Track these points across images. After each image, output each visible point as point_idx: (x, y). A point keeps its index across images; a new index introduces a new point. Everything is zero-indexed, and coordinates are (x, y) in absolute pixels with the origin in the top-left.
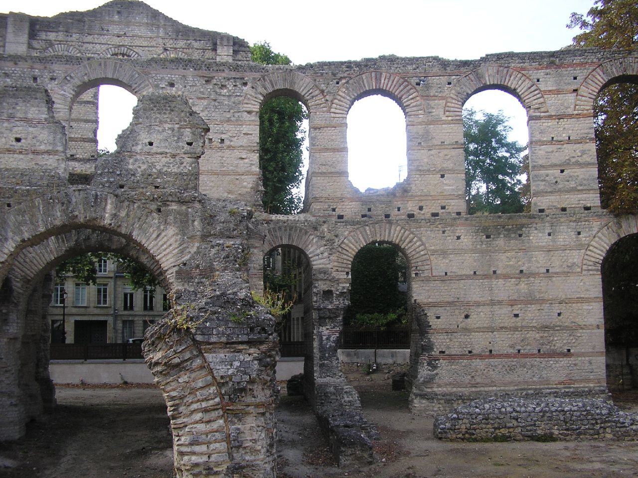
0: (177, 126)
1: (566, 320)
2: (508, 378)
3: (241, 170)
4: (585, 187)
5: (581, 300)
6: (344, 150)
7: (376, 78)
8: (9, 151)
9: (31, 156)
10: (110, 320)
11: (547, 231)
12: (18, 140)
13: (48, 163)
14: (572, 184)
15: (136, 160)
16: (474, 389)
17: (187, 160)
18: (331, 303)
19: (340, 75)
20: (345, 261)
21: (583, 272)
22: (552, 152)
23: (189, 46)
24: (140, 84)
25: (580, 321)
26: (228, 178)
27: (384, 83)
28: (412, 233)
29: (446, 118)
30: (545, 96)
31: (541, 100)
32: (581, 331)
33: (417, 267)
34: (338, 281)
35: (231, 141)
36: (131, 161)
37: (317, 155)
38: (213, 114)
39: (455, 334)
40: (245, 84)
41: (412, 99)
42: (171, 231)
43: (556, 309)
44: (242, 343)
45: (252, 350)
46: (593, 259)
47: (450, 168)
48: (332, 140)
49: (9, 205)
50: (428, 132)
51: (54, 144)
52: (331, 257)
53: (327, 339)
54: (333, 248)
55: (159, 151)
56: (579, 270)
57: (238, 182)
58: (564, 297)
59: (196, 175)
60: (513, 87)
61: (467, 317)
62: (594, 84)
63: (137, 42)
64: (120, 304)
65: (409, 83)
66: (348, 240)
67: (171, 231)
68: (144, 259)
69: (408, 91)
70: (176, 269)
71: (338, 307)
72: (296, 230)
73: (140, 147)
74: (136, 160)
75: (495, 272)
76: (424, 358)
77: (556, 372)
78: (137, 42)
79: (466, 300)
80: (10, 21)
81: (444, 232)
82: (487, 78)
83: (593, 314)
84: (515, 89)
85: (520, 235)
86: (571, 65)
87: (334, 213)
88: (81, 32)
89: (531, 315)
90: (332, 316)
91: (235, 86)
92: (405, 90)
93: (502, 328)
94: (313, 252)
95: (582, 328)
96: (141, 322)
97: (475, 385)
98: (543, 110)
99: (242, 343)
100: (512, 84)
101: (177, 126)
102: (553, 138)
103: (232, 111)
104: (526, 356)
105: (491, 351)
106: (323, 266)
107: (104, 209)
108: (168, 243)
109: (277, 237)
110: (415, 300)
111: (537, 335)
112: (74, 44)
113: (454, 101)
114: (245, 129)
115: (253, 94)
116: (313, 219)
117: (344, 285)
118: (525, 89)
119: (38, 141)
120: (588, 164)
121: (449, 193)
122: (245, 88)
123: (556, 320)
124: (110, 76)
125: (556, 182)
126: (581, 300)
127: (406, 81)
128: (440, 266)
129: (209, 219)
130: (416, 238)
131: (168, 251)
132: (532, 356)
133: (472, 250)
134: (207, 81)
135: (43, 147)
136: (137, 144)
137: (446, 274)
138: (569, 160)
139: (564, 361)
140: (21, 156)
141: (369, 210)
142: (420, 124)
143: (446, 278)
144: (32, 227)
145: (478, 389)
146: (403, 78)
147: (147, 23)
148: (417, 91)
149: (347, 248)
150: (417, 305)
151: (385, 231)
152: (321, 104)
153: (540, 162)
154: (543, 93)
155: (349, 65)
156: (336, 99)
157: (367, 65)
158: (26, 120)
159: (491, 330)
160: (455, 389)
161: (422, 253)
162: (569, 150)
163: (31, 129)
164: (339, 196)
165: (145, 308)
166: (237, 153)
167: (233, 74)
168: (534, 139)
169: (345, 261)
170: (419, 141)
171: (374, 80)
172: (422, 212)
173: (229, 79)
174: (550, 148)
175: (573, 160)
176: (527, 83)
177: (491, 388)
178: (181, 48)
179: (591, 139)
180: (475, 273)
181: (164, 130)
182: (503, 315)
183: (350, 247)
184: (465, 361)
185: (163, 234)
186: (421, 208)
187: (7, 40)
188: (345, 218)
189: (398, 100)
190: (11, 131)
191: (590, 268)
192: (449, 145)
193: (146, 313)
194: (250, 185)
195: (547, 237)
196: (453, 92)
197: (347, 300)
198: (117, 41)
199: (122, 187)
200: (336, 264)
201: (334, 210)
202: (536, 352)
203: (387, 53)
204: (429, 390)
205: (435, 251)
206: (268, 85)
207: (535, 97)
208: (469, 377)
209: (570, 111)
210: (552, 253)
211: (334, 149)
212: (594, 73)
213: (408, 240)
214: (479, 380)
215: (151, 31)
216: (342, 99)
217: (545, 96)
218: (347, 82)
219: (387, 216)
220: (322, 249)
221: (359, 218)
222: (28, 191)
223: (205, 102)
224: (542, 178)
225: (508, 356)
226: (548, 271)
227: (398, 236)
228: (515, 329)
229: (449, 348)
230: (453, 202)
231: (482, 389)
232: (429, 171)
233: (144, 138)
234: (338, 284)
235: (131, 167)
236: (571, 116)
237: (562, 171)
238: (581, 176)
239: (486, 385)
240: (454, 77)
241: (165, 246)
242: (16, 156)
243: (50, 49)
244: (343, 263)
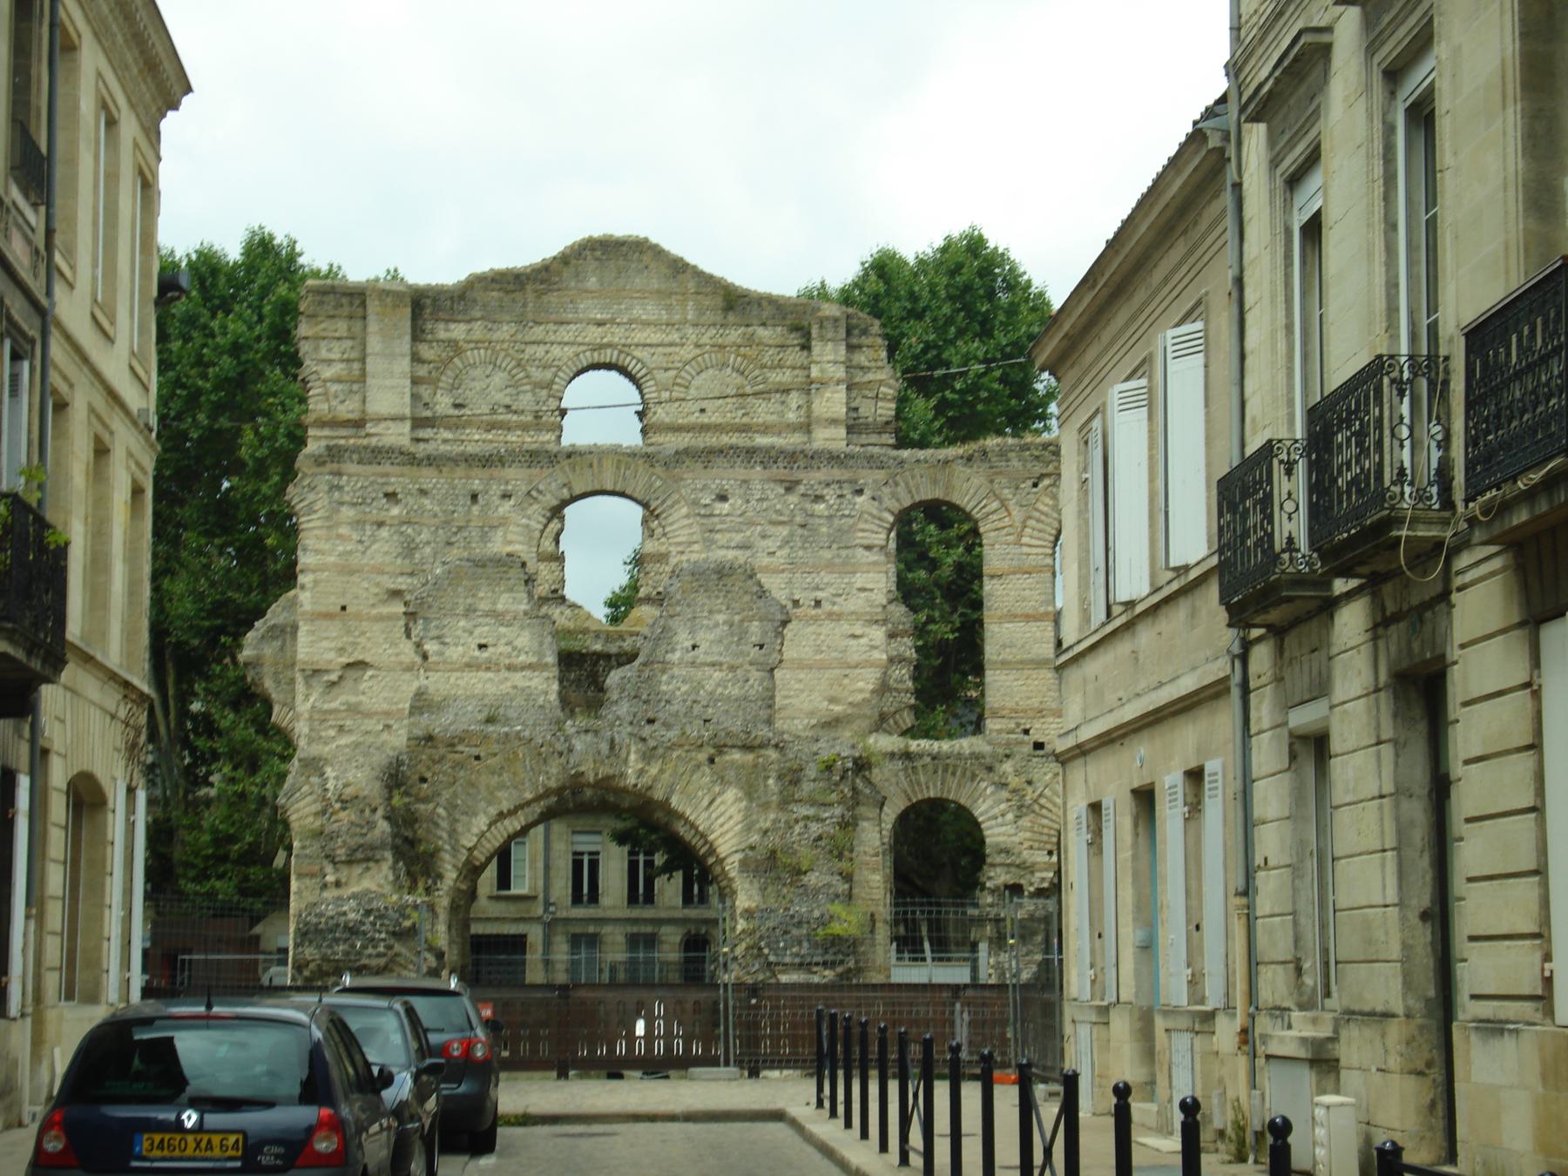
0: (737, 618)
3: (855, 658)
8: (468, 665)
9: (504, 674)
10: (535, 934)
12: (482, 647)
13: (534, 683)
15: (673, 677)
17: (755, 675)
19: (1038, 469)
23: (750, 341)
24: (664, 502)
26: (828, 674)
34: (1029, 868)
35: (834, 604)
36: (665, 678)
38: (801, 553)
40: (860, 492)
42: (731, 794)
44: (817, 964)
45: (827, 973)
48: (1024, 599)
49: (477, 758)
51: (541, 654)
52: (1020, 823)
55: (709, 659)
57: (846, 681)
59: (769, 701)
63: (639, 336)
64: (562, 888)
67: (731, 794)
68: (682, 830)
70: (739, 856)
72: (954, 774)
73: (678, 654)
74: (673, 677)
78: (639, 336)
80: (373, 307)
88: (520, 321)
91: (841, 496)
94: (986, 811)
96: (621, 939)
99: (817, 964)
101: (737, 618)
103: (835, 546)
107: (626, 761)
108: (727, 815)
109: (919, 784)
112: (505, 346)
114: (860, 580)
115: (875, 512)
116: (987, 749)
119: (514, 648)
122: (859, 500)
124: (609, 487)
129: (792, 777)
131: (726, 827)
134: (789, 490)
135: (522, 658)
136: (673, 651)
140: (490, 675)
144: (514, 792)
147: (658, 292)
149: (1049, 806)
156: (1030, 518)
158: (496, 615)
163: (502, 630)
165: (633, 899)
166: (845, 628)
167: (837, 473)
173: (828, 485)
178: (734, 344)
181: (717, 625)
185: (719, 800)
187: (369, 350)
188: (1048, 748)
190: (471, 633)
193: (636, 913)
194: (871, 687)
198: (593, 334)
199: (651, 721)
200: (1028, 835)
201: (1026, 732)
206: (901, 489)
215: (669, 308)
220: (1003, 806)
222: (507, 734)
223: (784, 531)
233: (683, 639)
234: (1032, 873)
235: (664, 688)
241: (723, 821)
242: (480, 674)
243: (456, 360)
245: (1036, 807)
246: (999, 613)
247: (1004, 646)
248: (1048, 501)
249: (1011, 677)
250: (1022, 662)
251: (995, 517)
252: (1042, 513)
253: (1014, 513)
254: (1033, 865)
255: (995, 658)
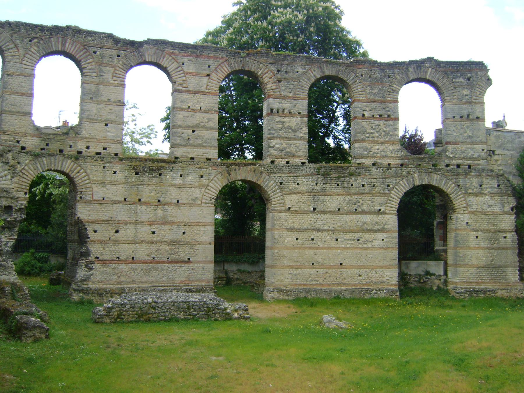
1: (188, 238)
2: (145, 278)
4: (208, 145)
5: (199, 224)
6: (31, 95)
7: (62, 43)
11: (179, 173)
14: (199, 142)
16: (119, 286)
18: (11, 216)
19: (33, 35)
20: (24, 184)
21: (203, 205)
22: (188, 117)
25: (198, 238)
27: (69, 47)
28: (80, 166)
29: (113, 82)
30: (187, 76)
31: (184, 78)
32: (198, 246)
33: (81, 192)
34: (17, 199)
37: (8, 97)
39: (108, 245)
41: (88, 63)
43: (182, 229)
46: (210, 196)
47: (113, 119)
48: (22, 86)
50: (98, 90)
52: (13, 180)
53: (5, 245)
54: (16, 173)
56: (200, 202)
58: (188, 221)
60: (165, 66)
61: (117, 232)
62: (221, 73)
65: (88, 51)
66: (28, 167)
69: (87, 57)
71: (16, 219)
75: (140, 200)
76: (82, 262)
77: (179, 274)
79: (117, 219)
81: (104, 167)
82: (147, 57)
83: (207, 235)
84: (166, 68)
85: (160, 175)
86: (208, 57)
87: (18, 144)
89: (165, 233)
90: (10, 226)
92: (84, 56)
93: (142, 241)
95: (199, 244)
97: (120, 283)
98: (184, 85)
100: (164, 63)
102: (189, 107)
104: (158, 262)
105: (133, 258)
106: (6, 186)
110: (78, 217)
111: (168, 247)
113: (120, 70)
117: (23, 202)
118: (173, 68)
120: (211, 129)
121: (110, 138)
123: (181, 238)
125: (189, 139)
126: (199, 224)
127: (85, 49)
128: (99, 192)
130: (82, 171)
132: (163, 262)
133: (125, 183)
137: (103, 199)
138: (199, 124)
139: (186, 267)
141: (47, 145)
142: (93, 83)
143: (103, 201)
145: (122, 286)
146: (84, 46)
148: (93, 58)
149: (27, 174)
150: (79, 222)
151: (59, 163)
152: (15, 56)
153: (179, 123)
154: (186, 74)
155: (42, 28)
157: (56, 30)
159: (134, 242)
160: (105, 286)
161: (87, 182)
162: (199, 117)
164: (23, 131)
168: (176, 106)
169: (24, 184)
170: (91, 96)
171: (60, 44)
172: (88, 151)
174: (186, 114)
175: (202, 124)
176: (175, 65)
177: (132, 285)
179: (216, 111)
180: (125, 199)
182: (144, 232)
183: (29, 173)
184: (114, 265)
186: (88, 148)
189: (78, 63)
191: (207, 201)
192: (114, 102)
195: (179, 177)
196: (121, 62)
197: (24, 214)
200: (16, 185)
202: (165, 259)
203: (73, 24)
204: (85, 286)
205: (97, 181)
207: (180, 76)
208: (116, 277)
209: (203, 89)
210: (182, 189)
211: (23, 94)
212: (222, 65)
213: (76, 171)
214: (123, 279)
216: (33, 54)
217: (187, 76)
218: (38, 42)
219: (61, 151)
221: (38, 151)
224: (179, 135)
225: (145, 262)
226: (178, 202)
227: (68, 167)
228: (152, 243)
229: (102, 255)
230: (113, 146)
231: (125, 286)
232: (97, 120)
234: (17, 201)
236: (203, 93)
237: (194, 131)
238: (206, 137)
239: (128, 283)
240: (122, 52)
244: (22, 185)
245: (21, 174)
246: (10, 90)
247: (11, 105)
248: (35, 48)
249: (13, 118)
250: (19, 112)
251: (12, 51)
252: (33, 52)
253: (20, 50)
254: (18, 198)
255: (7, 109)
